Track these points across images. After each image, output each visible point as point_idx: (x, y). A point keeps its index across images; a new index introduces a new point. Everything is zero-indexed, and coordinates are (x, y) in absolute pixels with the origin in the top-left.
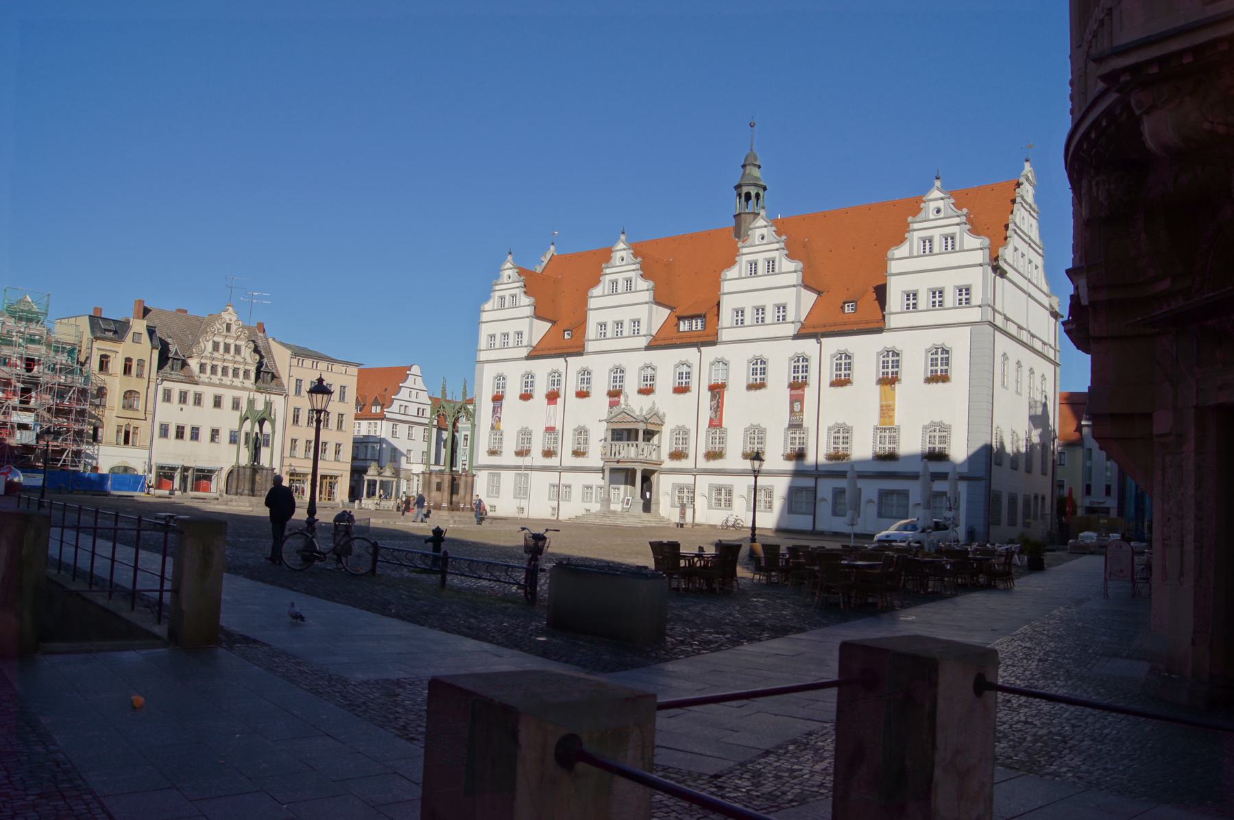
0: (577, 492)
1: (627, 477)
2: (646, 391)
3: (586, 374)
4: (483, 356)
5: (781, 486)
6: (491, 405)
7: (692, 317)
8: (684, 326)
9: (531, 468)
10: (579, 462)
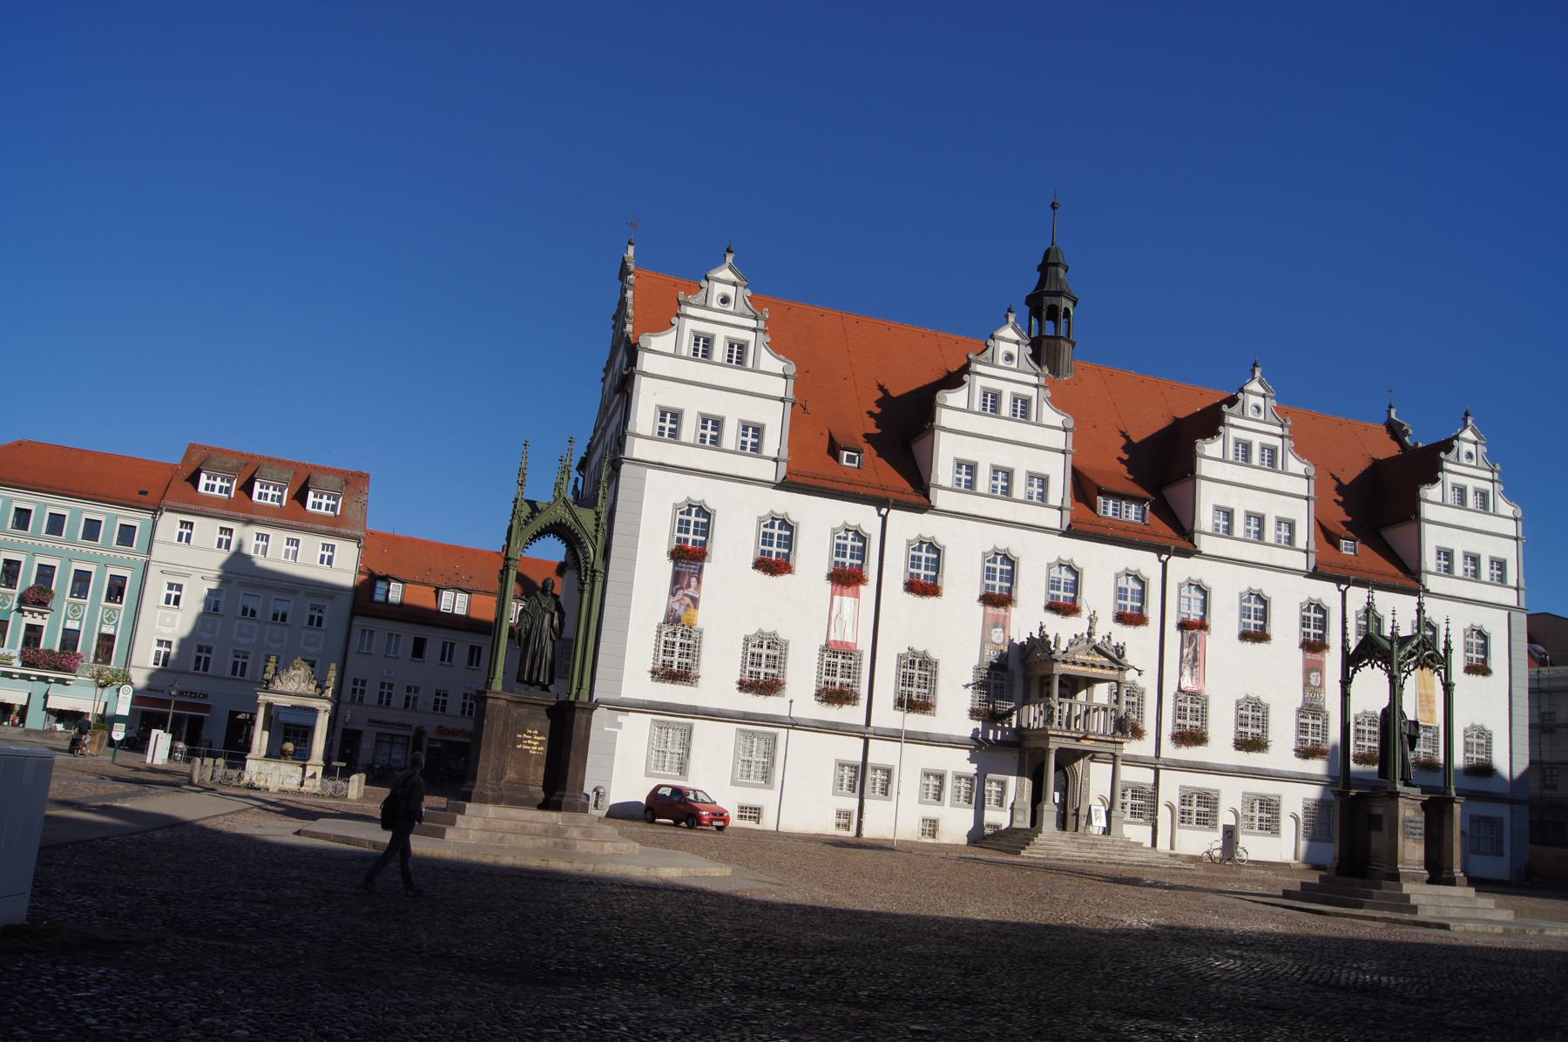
0: (909, 784)
1: (1021, 761)
2: (1063, 608)
3: (931, 553)
4: (638, 448)
5: (1297, 799)
6: (668, 567)
9: (794, 724)
10: (915, 722)
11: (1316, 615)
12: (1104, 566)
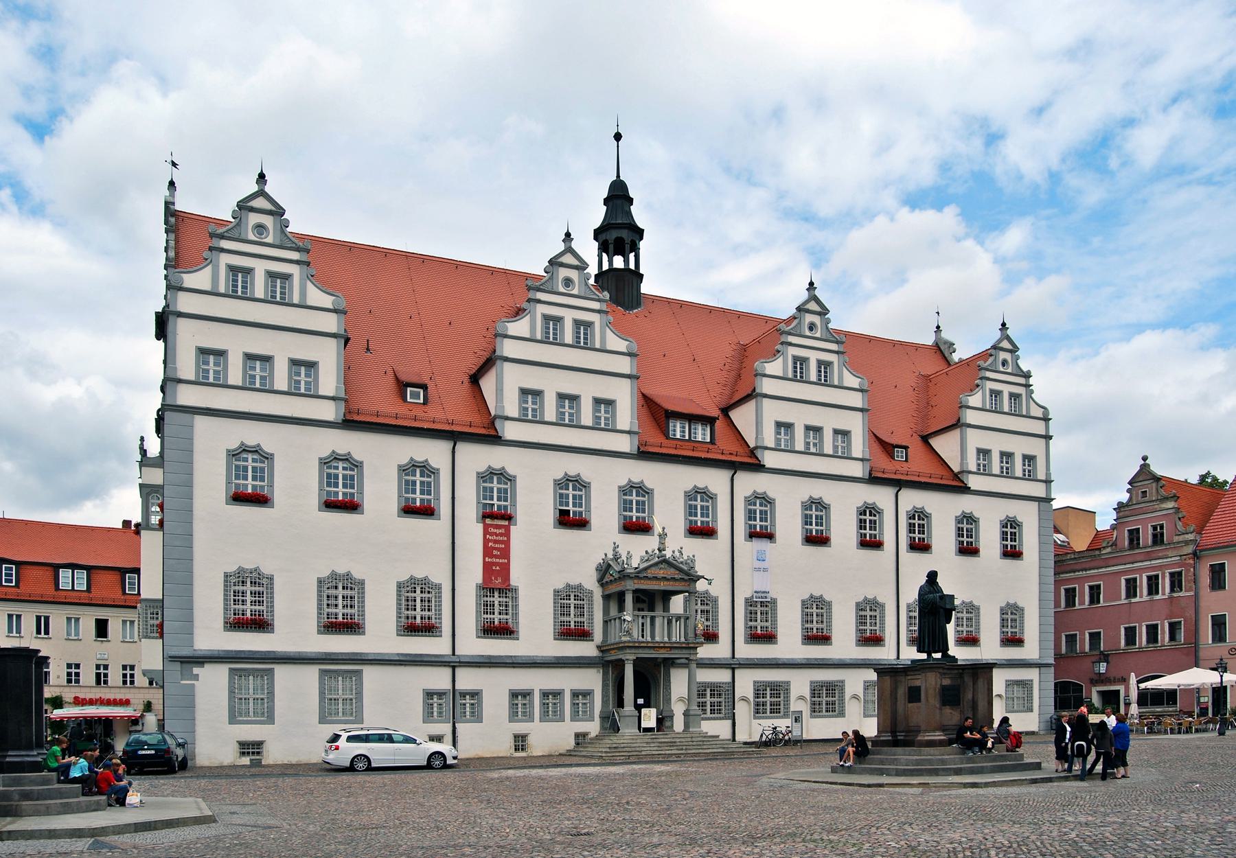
0: (495, 702)
7: (692, 419)
8: (678, 429)
11: (868, 515)
12: (670, 485)
